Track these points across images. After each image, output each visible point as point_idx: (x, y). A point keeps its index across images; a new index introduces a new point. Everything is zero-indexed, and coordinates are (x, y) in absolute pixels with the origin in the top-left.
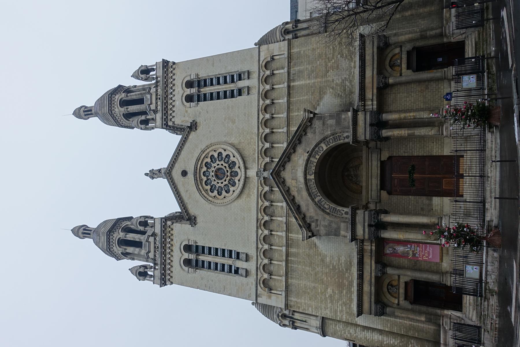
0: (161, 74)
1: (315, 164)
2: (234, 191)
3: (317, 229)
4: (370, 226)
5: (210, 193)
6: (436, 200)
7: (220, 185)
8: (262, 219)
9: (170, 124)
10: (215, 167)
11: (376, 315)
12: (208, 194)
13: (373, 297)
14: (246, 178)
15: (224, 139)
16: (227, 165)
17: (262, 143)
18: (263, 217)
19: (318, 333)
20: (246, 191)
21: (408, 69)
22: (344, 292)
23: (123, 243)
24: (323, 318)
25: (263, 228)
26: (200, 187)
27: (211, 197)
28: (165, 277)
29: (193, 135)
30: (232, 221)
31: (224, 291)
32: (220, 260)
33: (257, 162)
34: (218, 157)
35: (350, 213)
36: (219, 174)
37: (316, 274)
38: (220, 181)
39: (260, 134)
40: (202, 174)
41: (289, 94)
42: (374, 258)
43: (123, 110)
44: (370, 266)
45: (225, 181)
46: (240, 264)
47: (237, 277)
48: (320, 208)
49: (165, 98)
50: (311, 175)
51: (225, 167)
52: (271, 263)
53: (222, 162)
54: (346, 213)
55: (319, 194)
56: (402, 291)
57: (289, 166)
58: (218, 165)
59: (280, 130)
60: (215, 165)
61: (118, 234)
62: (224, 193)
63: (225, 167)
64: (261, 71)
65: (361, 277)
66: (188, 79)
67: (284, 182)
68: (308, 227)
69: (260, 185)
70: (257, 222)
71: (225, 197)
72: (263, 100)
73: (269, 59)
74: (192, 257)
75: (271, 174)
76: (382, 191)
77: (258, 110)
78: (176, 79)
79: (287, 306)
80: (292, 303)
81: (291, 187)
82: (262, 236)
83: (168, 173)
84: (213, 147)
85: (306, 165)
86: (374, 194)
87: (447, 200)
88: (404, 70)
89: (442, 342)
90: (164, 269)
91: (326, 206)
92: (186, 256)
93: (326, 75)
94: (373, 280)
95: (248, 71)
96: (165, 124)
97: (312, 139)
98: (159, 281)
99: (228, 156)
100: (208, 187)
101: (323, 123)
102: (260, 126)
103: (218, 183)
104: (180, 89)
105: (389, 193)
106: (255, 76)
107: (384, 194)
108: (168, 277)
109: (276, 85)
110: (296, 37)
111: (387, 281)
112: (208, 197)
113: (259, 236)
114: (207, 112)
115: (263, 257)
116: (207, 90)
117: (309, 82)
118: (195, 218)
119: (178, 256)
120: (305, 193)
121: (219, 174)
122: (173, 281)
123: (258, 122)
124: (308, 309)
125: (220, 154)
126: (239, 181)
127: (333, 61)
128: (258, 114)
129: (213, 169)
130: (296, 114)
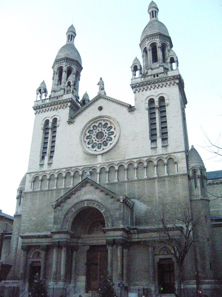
1: (93, 206)
4: (59, 242)
7: (93, 136)
8: (72, 171)
10: (104, 131)
11: (22, 246)
15: (122, 135)
16: (105, 140)
18: (73, 171)
20: (88, 157)
21: (160, 259)
24: (21, 215)
25: (67, 172)
26: (92, 122)
27: (85, 132)
28: (39, 109)
29: (125, 110)
30: (71, 150)
35: (65, 230)
36: (100, 135)
38: (95, 137)
40: (100, 122)
41: (150, 179)
44: (44, 242)
49: (151, 82)
51: (104, 139)
54: (65, 228)
56: (35, 260)
57: (92, 188)
58: (106, 133)
60: (105, 131)
61: (65, 65)
62: (88, 140)
64: (167, 156)
65: (39, 237)
66: (166, 98)
71: (85, 142)
72: (146, 161)
75: (87, 178)
76: (89, 247)
79: (26, 193)
80: (27, 197)
82: (62, 172)
83: (100, 96)
87: (84, 284)
90: (42, 107)
91: (69, 216)
94: (38, 244)
95: (167, 146)
97: (109, 202)
98: (36, 105)
103: (94, 135)
104: (159, 93)
105: (88, 251)
107: (87, 248)
108: (38, 111)
109: (157, 169)
110: (189, 178)
112: (85, 129)
115: (51, 174)
116: (157, 115)
117: (157, 193)
118: (73, 123)
120: (76, 201)
121: (100, 135)
123: (132, 159)
126: (95, 150)
129: (103, 130)
130: (136, 186)
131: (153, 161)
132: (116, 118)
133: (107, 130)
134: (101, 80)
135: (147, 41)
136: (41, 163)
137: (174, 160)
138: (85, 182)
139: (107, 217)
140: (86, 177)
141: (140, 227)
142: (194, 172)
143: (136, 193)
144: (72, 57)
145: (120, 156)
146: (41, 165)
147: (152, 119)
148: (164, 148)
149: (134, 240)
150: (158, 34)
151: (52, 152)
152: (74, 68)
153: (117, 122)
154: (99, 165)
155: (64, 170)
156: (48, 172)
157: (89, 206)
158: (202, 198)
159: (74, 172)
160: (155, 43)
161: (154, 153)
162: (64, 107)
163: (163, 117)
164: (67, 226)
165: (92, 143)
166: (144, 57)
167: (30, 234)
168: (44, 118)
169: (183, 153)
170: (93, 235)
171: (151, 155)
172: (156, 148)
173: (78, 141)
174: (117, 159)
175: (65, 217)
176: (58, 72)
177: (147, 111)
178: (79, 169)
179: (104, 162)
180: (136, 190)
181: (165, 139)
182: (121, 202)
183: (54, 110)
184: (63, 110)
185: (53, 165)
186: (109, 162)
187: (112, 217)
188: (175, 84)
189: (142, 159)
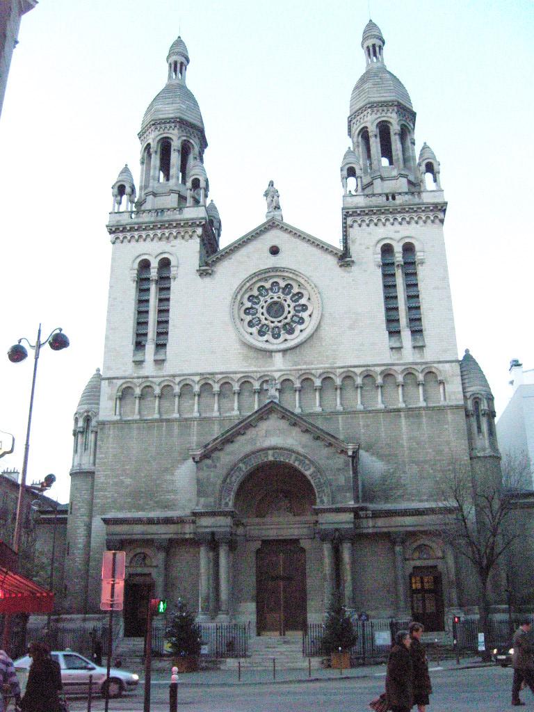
1: (287, 461)
2: (251, 334)
3: (205, 468)
4: (213, 534)
5: (247, 296)
6: (252, 606)
7: (260, 310)
8: (215, 382)
10: (285, 300)
12: (246, 292)
13: (129, 537)
14: (269, 353)
16: (288, 320)
17: (320, 376)
18: (218, 382)
19: (73, 466)
20: (252, 354)
21: (414, 568)
22: (129, 500)
23: (165, 146)
24: (94, 473)
25: (203, 382)
27: (242, 297)
28: (122, 231)
29: (332, 261)
30: (208, 333)
31: (112, 329)
32: (152, 318)
33: (295, 367)
34: (299, 305)
36: (275, 309)
37: (149, 462)
38: (264, 311)
41: (390, 411)
42: (175, 537)
43: (373, 130)
45: (266, 319)
46: (150, 347)
47: (132, 347)
48: (232, 470)
50: (273, 456)
53: (293, 312)
54: (227, 504)
55: (249, 468)
56: (139, 570)
57: (283, 424)
58: (289, 306)
59: (338, 400)
62: (249, 318)
63: (286, 318)
64: (424, 366)
65: (150, 522)
67: (261, 419)
68: (205, 456)
69: (262, 374)
71: (242, 320)
72: (382, 373)
74: (154, 273)
76: (260, 542)
77: (369, 366)
78: (418, 226)
80: (106, 431)
81: (257, 429)
82: (191, 383)
83: (274, 223)
85: (286, 449)
86: (255, 532)
88: (413, 563)
89: (87, 616)
90: (132, 229)
91: (233, 479)
92: (154, 264)
93: (413, 462)
94: (149, 537)
97: (321, 454)
98: (114, 223)
99: (302, 321)
100: (255, 293)
101: (340, 469)
103: (262, 308)
105: (258, 552)
107: (258, 545)
108: (121, 236)
111: (147, 551)
112: (241, 293)
113: (191, 377)
115: (163, 385)
116: (400, 280)
118: (210, 274)
119: (152, 249)
120: (248, 449)
121: (275, 309)
122: (116, 244)
123: (351, 367)
124: (102, 453)
125: (304, 308)
126: (267, 341)
127: (431, 471)
132: (311, 276)
133: (291, 299)
134: (272, 185)
135: (371, 114)
136: (138, 358)
137: (436, 377)
138: (266, 412)
139: (320, 485)
140: (270, 400)
141: (371, 506)
142: (477, 403)
143: (362, 438)
144: (189, 117)
146: (139, 363)
147: (389, 287)
148: (416, 351)
149: (365, 531)
150: (396, 103)
151: (162, 334)
152: (195, 145)
153: (316, 286)
154: (279, 374)
155: (197, 378)
156: (157, 380)
157: (278, 460)
158: (492, 454)
159: (219, 385)
160: (389, 122)
161: (398, 359)
162: (187, 236)
163: (412, 286)
164: (229, 500)
165: (258, 325)
166: (358, 146)
167: (121, 515)
168: (137, 255)
169: (454, 364)
170: (267, 519)
171: (390, 362)
172: (400, 348)
173: (227, 318)
175: (224, 481)
176: (159, 150)
177: (380, 269)
178: (232, 379)
179: (289, 368)
180: (363, 431)
181: (417, 332)
182: (350, 456)
183: (160, 239)
184: (183, 241)
185: (166, 364)
186: (301, 370)
187: (331, 485)
188: (437, 221)
189: (372, 369)
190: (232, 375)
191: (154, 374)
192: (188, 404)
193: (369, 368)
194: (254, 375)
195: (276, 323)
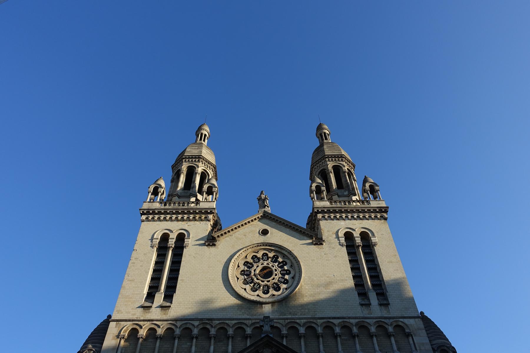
0: (372, 206)
8: (212, 326)
9: (320, 216)
17: (305, 324)
18: (215, 327)
25: (201, 326)
33: (282, 317)
39: (315, 321)
49: (347, 210)
52: (157, 338)
64: (392, 320)
69: (254, 321)
70: (208, 319)
72: (357, 324)
73: (407, 331)
82: (191, 327)
84: (295, 264)
95: (389, 304)
96: (318, 210)
102: (325, 320)
106: (385, 314)
114: (335, 257)
118: (214, 245)
123: (330, 318)
128: (338, 318)
131: (369, 327)
145: (307, 311)
148: (383, 307)
159: (216, 329)
174: (301, 315)
186: (287, 319)
190: (227, 322)
191: (159, 318)
192: (185, 346)
193: (345, 320)
194: (247, 322)
195: (266, 282)
